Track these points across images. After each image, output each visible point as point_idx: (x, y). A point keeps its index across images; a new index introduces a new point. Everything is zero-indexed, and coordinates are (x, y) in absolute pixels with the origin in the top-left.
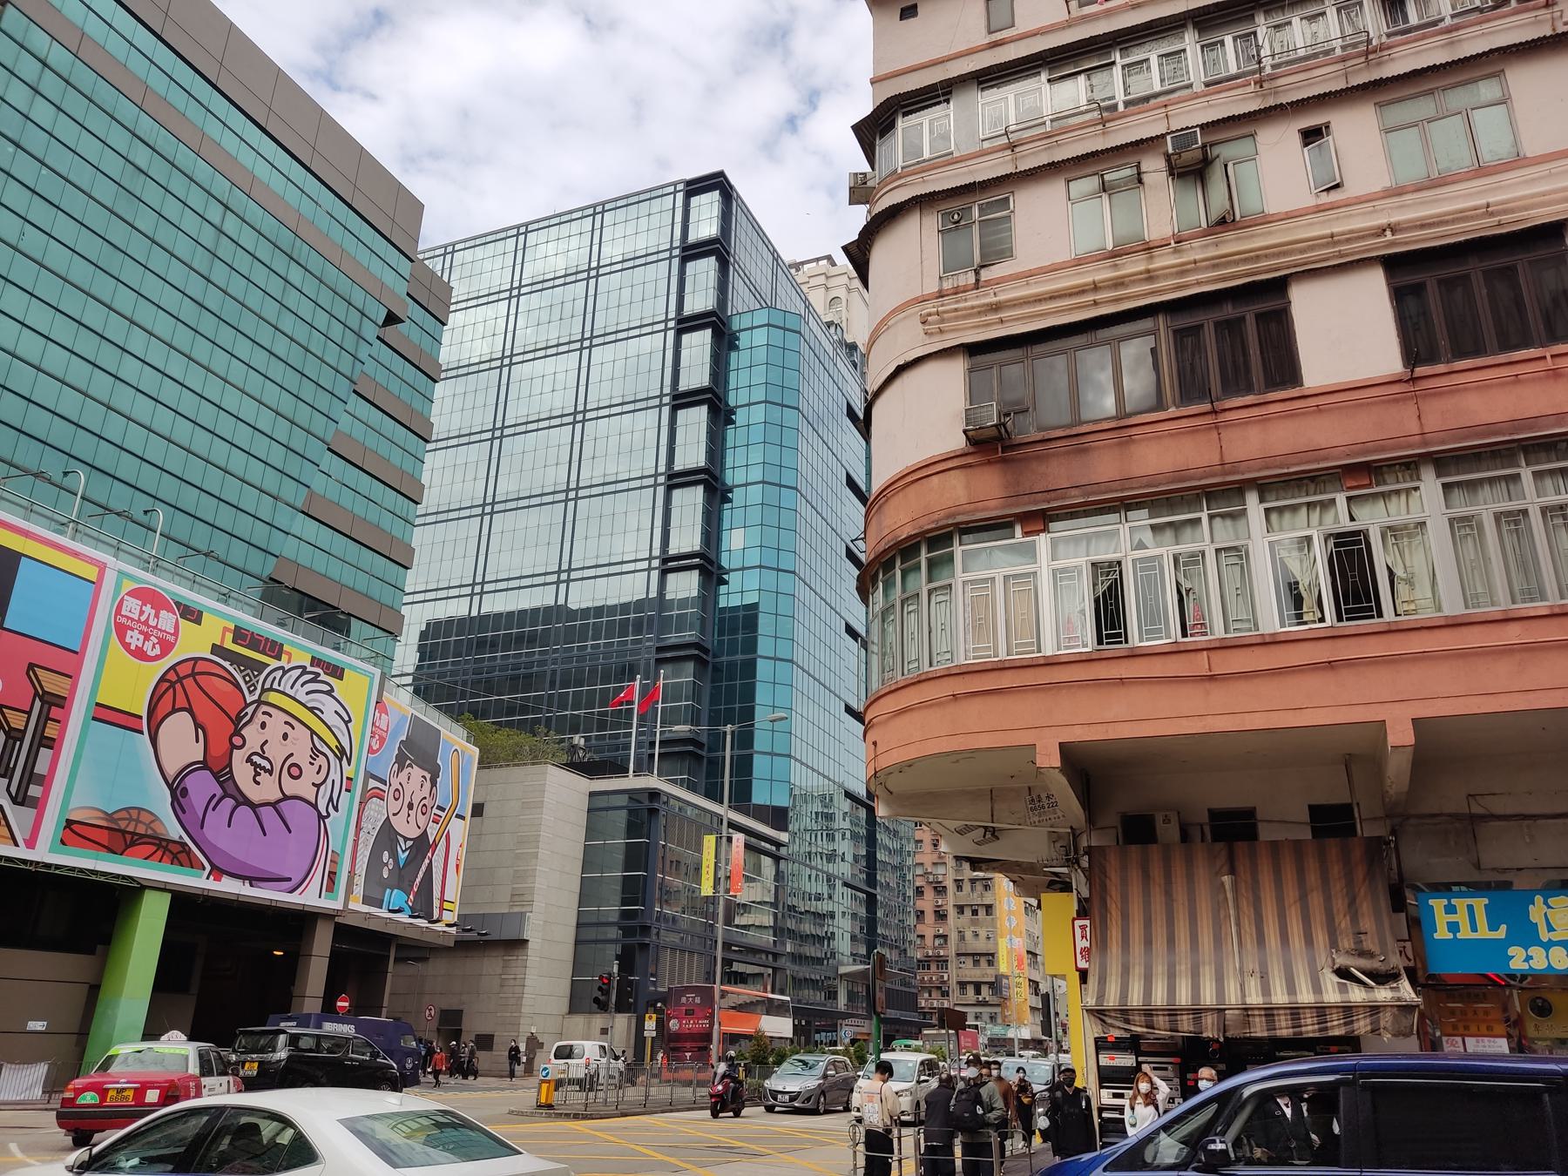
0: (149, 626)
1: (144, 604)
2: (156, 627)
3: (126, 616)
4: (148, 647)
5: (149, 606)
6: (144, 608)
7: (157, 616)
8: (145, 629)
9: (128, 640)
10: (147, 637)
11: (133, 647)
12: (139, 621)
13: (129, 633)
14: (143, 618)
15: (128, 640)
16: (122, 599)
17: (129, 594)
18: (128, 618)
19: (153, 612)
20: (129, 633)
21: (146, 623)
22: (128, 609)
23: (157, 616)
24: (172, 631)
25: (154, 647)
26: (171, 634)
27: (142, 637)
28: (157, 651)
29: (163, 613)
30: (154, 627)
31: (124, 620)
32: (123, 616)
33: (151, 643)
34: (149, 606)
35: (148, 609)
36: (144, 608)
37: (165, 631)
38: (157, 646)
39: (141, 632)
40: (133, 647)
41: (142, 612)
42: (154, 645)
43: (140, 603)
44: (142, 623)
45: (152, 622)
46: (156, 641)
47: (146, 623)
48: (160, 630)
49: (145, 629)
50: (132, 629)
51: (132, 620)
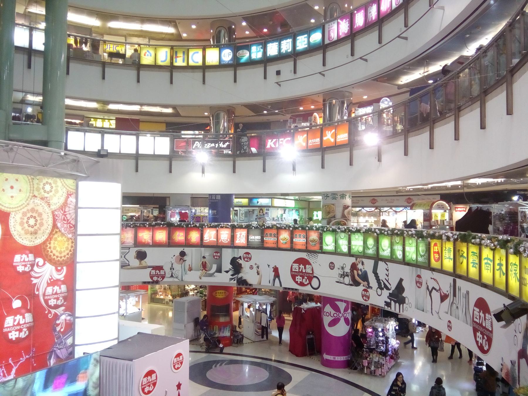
0: (303, 273)
1: (300, 265)
4: (304, 280)
5: (302, 265)
6: (300, 266)
7: (305, 268)
8: (301, 274)
9: (297, 280)
11: (299, 282)
13: (297, 277)
14: (300, 270)
15: (297, 280)
17: (294, 263)
19: (303, 267)
20: (297, 277)
23: (305, 268)
24: (311, 272)
25: (306, 281)
27: (301, 278)
31: (294, 273)
36: (300, 266)
37: (309, 273)
38: (307, 280)
40: (299, 282)
41: (299, 268)
42: (306, 279)
43: (298, 265)
44: (300, 272)
45: (304, 271)
46: (306, 278)
48: (308, 273)
50: (297, 276)
51: (297, 272)
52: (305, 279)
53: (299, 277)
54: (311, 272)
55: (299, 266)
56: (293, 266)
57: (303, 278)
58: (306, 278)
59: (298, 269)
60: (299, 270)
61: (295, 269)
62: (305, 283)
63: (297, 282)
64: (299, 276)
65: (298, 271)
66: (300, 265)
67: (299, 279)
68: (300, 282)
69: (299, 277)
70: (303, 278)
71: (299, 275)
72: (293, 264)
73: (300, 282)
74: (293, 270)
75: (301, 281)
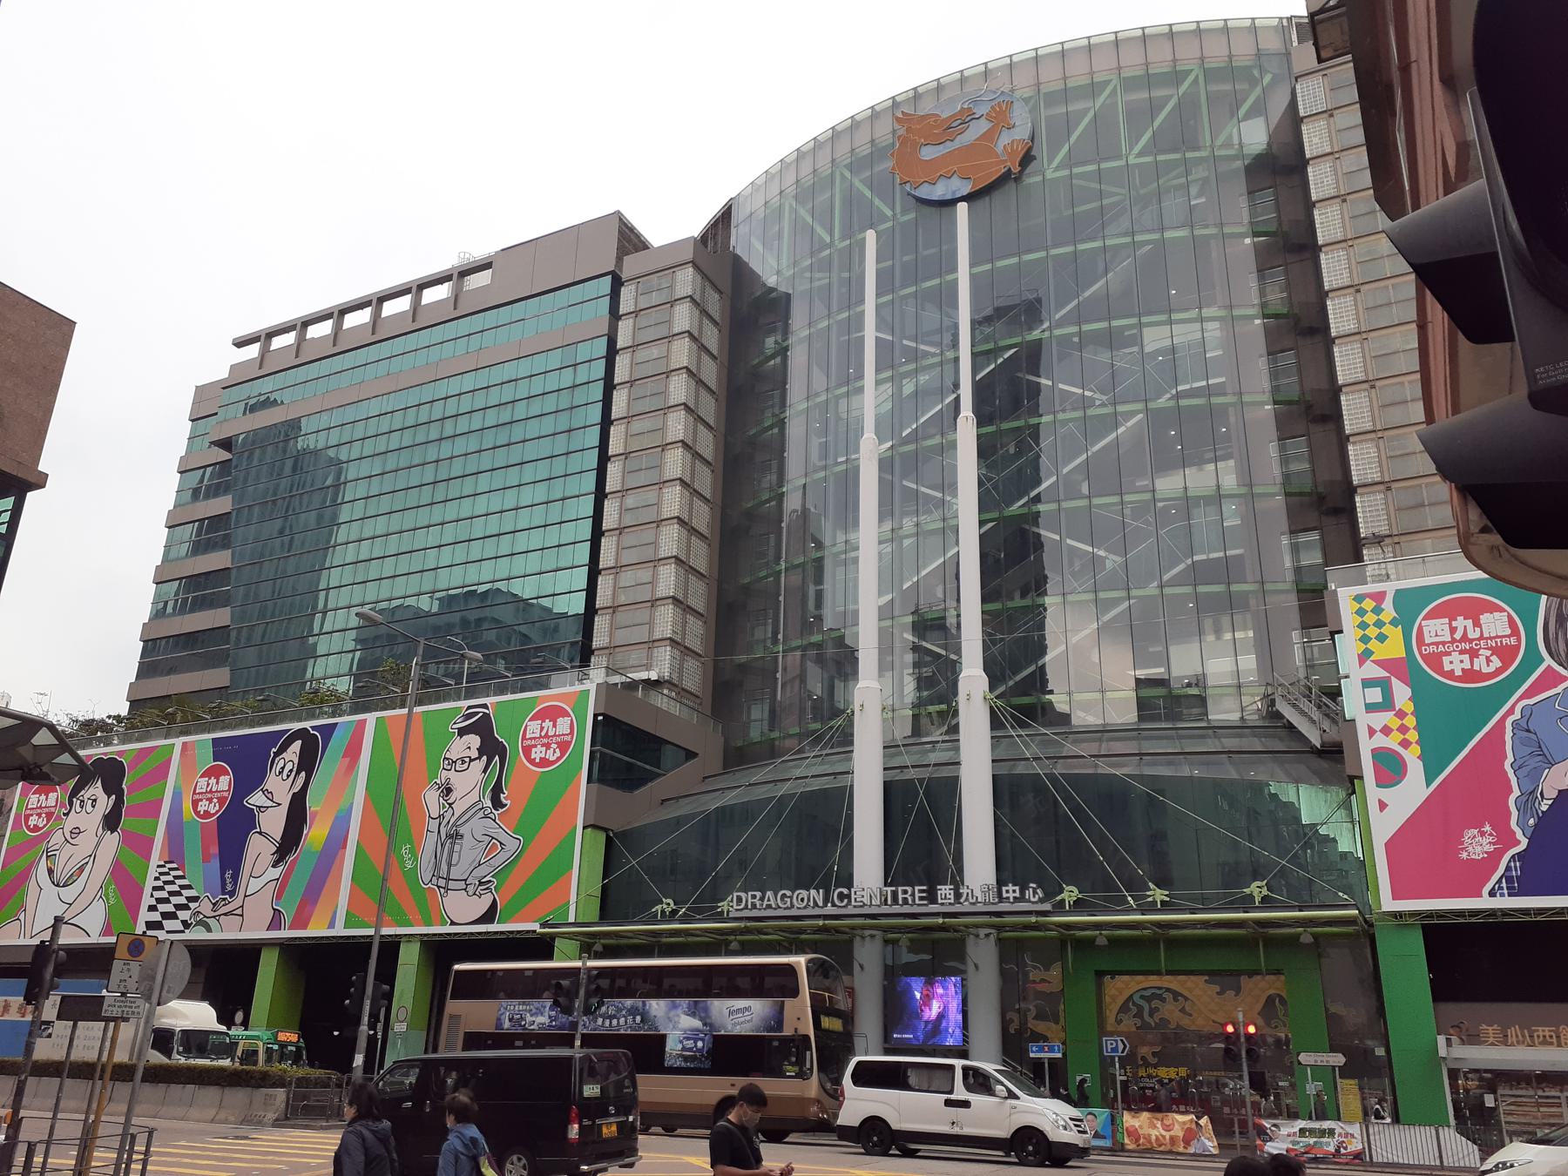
0: (1471, 641)
2: (1481, 638)
3: (1432, 644)
4: (1480, 664)
5: (1460, 618)
6: (1454, 624)
7: (1477, 624)
9: (1447, 667)
11: (1458, 673)
12: (1454, 641)
14: (1458, 636)
15: (1447, 667)
18: (1437, 644)
19: (1469, 623)
20: (1446, 660)
21: (1465, 638)
22: (1433, 634)
23: (1477, 624)
25: (1488, 660)
26: (1509, 636)
27: (1466, 657)
28: (1496, 663)
29: (1485, 618)
30: (1479, 639)
31: (1432, 649)
32: (1429, 645)
35: (1460, 623)
36: (1454, 624)
37: (1497, 637)
38: (1494, 658)
39: (1462, 652)
40: (1458, 673)
41: (1453, 630)
43: (1447, 620)
44: (1460, 641)
46: (1489, 653)
47: (1465, 638)
48: (1491, 638)
50: (1449, 654)
51: (1444, 643)
53: (1456, 657)
54: (1508, 632)
57: (1473, 654)
60: (1452, 637)
61: (1436, 635)
62: (1485, 670)
67: (1457, 662)
68: (1463, 669)
69: (1456, 657)
70: (1473, 654)
71: (1454, 651)
72: (1424, 623)
73: (1463, 669)
75: (1467, 666)
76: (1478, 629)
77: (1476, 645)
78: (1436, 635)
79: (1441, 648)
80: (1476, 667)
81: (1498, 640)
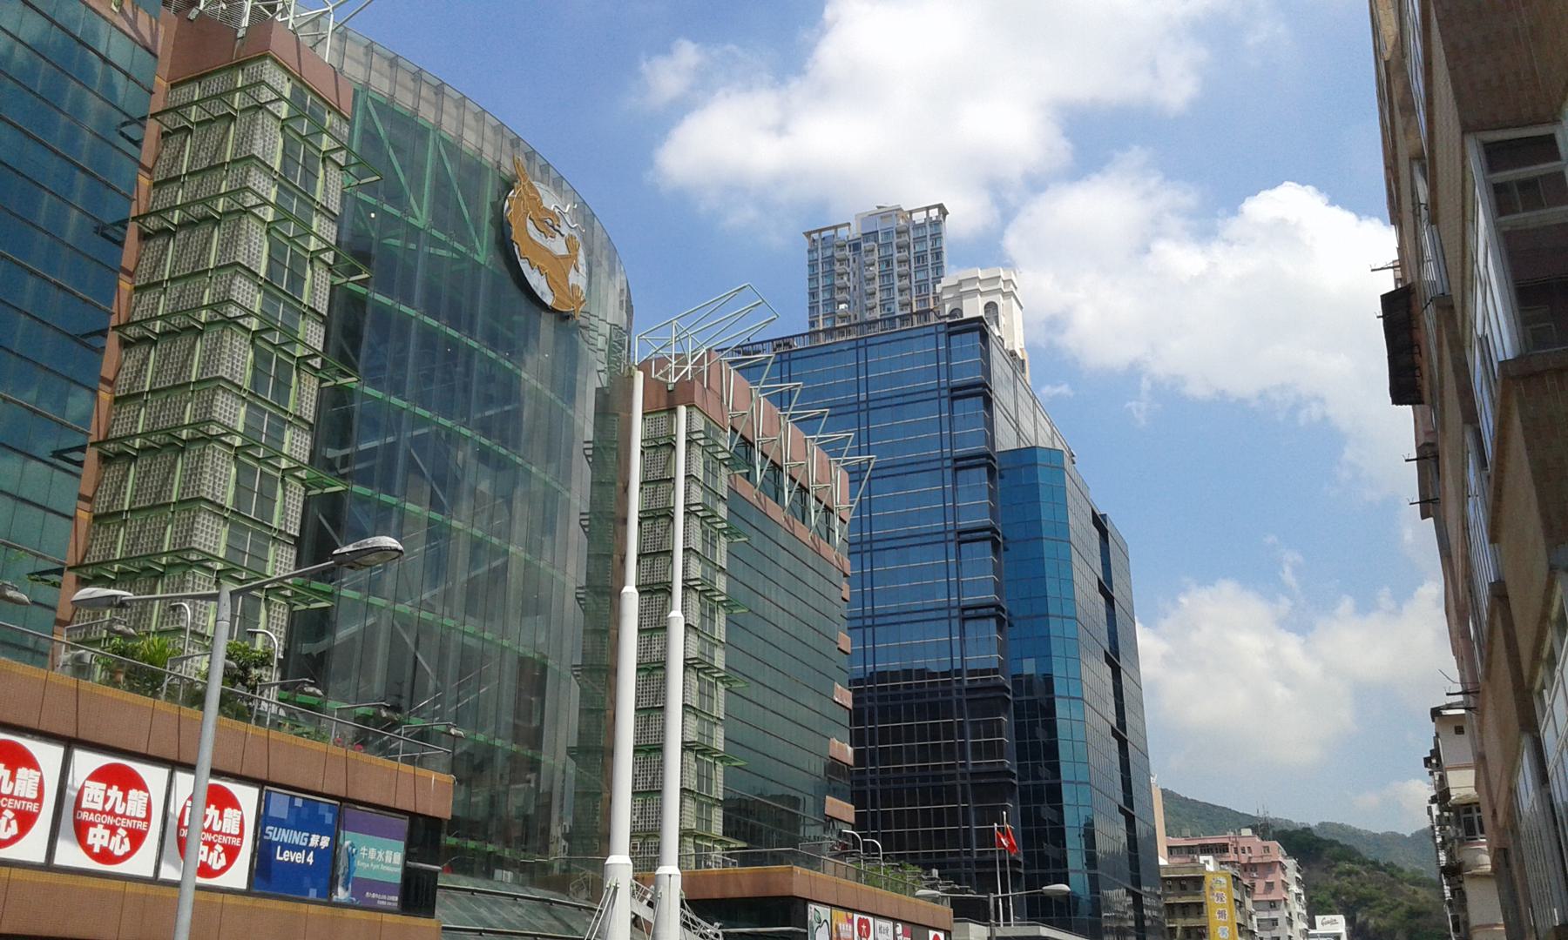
1: (109, 786)
5: (115, 788)
7: (125, 799)
8: (110, 820)
10: (113, 830)
11: (97, 850)
14: (108, 807)
15: (90, 841)
16: (83, 787)
18: (90, 811)
19: (120, 794)
20: (92, 831)
21: (112, 813)
22: (90, 799)
23: (125, 799)
25: (122, 842)
27: (107, 833)
28: (127, 847)
33: (118, 838)
34: (115, 788)
35: (115, 793)
36: (110, 792)
39: (106, 826)
41: (106, 799)
43: (104, 786)
45: (119, 810)
47: (112, 813)
49: (110, 820)
50: (94, 825)
51: (95, 812)
52: (118, 838)
55: (106, 792)
56: (86, 790)
58: (122, 832)
59: (101, 800)
61: (93, 801)
63: (88, 849)
64: (100, 827)
65: (99, 808)
66: (111, 788)
67: (99, 836)
72: (89, 783)
74: (85, 804)
76: (124, 804)
77: (5, 802)
78: (93, 801)
79: (92, 818)
80: (111, 848)
81: (24, 802)
